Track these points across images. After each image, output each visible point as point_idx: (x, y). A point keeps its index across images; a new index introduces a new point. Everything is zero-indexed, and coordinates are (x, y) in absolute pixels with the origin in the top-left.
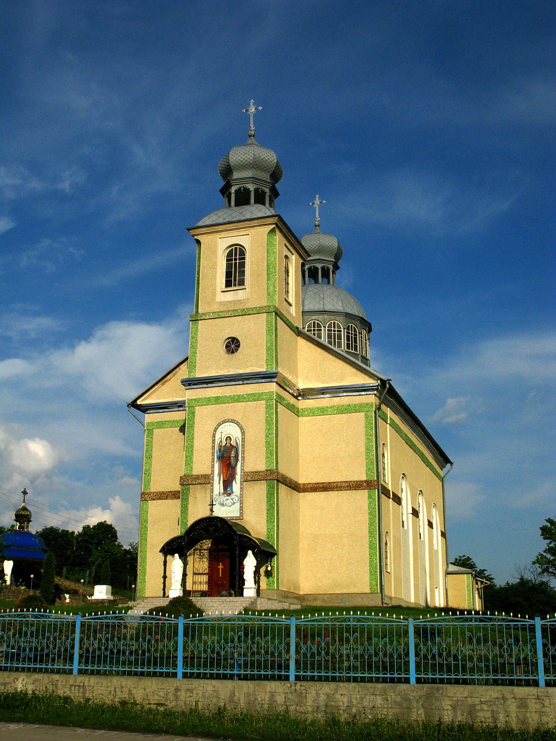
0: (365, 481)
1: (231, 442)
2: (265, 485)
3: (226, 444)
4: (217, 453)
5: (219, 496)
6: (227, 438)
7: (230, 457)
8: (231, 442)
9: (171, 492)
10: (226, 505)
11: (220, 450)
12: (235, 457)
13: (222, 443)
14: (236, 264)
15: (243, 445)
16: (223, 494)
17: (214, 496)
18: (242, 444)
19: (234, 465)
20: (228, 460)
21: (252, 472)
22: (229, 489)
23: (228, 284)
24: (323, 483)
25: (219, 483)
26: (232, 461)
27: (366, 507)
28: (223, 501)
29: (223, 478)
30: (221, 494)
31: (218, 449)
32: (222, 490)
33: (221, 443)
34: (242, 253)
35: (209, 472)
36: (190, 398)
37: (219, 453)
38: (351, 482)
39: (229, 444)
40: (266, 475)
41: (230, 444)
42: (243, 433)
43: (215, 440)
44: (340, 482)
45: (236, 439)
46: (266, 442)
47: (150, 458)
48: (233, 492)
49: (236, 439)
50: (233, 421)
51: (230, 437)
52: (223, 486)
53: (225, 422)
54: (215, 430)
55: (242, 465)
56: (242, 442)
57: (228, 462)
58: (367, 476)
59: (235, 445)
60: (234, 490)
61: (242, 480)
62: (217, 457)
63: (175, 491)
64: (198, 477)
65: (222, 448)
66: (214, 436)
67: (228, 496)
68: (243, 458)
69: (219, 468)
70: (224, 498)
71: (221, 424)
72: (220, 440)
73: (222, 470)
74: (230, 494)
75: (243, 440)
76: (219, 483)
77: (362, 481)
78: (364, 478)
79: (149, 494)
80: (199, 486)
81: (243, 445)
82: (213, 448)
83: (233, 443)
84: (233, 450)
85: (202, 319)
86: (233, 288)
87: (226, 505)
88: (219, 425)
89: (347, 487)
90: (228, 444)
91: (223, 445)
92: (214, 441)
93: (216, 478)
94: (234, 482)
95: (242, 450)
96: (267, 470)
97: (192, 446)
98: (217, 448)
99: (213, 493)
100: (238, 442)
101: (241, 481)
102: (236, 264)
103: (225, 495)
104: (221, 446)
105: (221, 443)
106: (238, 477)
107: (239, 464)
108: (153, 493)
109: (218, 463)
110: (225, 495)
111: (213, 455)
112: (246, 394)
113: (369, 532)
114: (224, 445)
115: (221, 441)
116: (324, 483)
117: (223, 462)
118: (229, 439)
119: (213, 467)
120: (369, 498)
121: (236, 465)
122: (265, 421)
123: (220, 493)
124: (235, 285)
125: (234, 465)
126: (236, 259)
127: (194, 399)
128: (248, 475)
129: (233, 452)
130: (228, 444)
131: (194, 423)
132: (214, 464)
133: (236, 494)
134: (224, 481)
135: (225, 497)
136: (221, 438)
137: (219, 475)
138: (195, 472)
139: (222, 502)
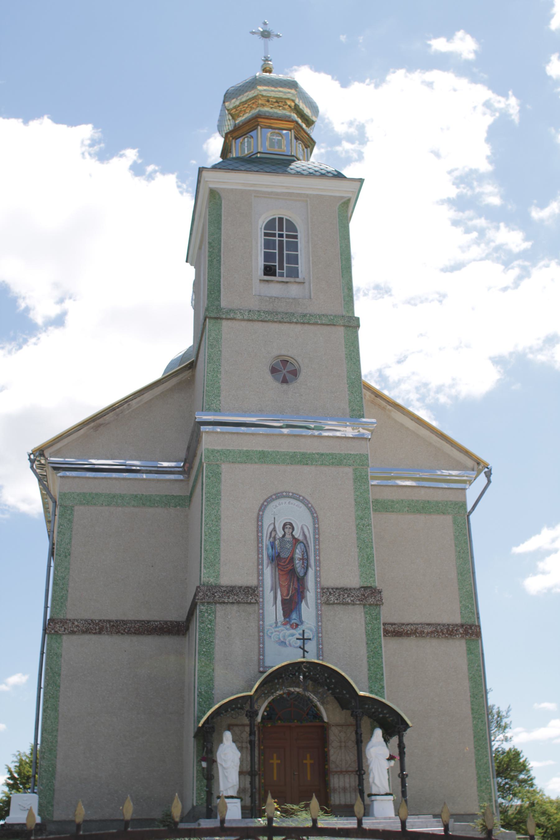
0: (462, 626)
1: (294, 533)
2: (363, 614)
3: (284, 536)
4: (268, 549)
5: (276, 626)
6: (285, 525)
7: (292, 559)
8: (294, 533)
9: (109, 621)
10: (290, 645)
11: (273, 545)
12: (303, 559)
13: (276, 534)
14: (281, 242)
15: (317, 540)
16: (285, 624)
17: (267, 628)
18: (315, 538)
19: (302, 574)
20: (289, 563)
21: (337, 589)
22: (294, 616)
23: (269, 271)
24: (392, 624)
25: (275, 603)
26: (297, 566)
27: (465, 667)
28: (284, 637)
29: (282, 595)
30: (279, 624)
31: (268, 543)
32: (281, 618)
33: (273, 535)
34: (291, 226)
35: (252, 581)
36: (210, 447)
37: (270, 550)
38: (439, 625)
39: (291, 536)
40: (364, 595)
41: (293, 536)
42: (316, 519)
43: (262, 525)
44: (421, 624)
45: (302, 528)
46: (358, 538)
47: (66, 557)
48: (302, 622)
49: (302, 528)
50: (296, 497)
51: (291, 524)
52: (283, 609)
53: (279, 496)
54: (263, 508)
55: (317, 576)
56: (314, 535)
57: (290, 567)
58: (462, 617)
59: (301, 538)
60: (304, 618)
61: (319, 601)
62: (268, 556)
63: (117, 621)
64: (231, 590)
65: (277, 542)
66: (260, 519)
67: (293, 628)
68: (318, 563)
69: (274, 577)
70: (286, 631)
71: (273, 500)
72: (272, 527)
73: (279, 579)
74: (297, 625)
75: (317, 531)
76: (275, 603)
77: (457, 625)
78: (458, 620)
79: (64, 622)
80: (235, 607)
81: (317, 540)
82: (259, 540)
83: (297, 534)
84: (299, 547)
85: (228, 317)
86: (277, 278)
87: (290, 645)
88: (269, 500)
89: (432, 632)
90: (288, 537)
91: (277, 537)
92: (259, 528)
93: (268, 595)
94: (303, 604)
95: (315, 549)
96: (365, 588)
97: (217, 533)
98: (266, 541)
99: (263, 621)
100: (307, 533)
101: (317, 603)
102: (281, 242)
103: (288, 627)
104: (275, 538)
105: (273, 535)
106: (311, 595)
107: (311, 573)
108: (73, 621)
109: (269, 569)
110: (288, 627)
111: (259, 551)
112: (318, 454)
113: (472, 709)
114: (281, 536)
115: (274, 529)
116: (395, 624)
117: (280, 567)
118: (288, 526)
119: (260, 574)
120: (468, 654)
121: (306, 573)
122: (353, 503)
123: (276, 623)
124: (282, 275)
125: (302, 574)
126: (281, 236)
127: (218, 451)
128: (330, 593)
129: (297, 551)
130: (288, 537)
131: (219, 492)
132: (262, 569)
133: (308, 626)
134: (284, 602)
135: (287, 629)
136: (274, 523)
137: (274, 589)
138: (226, 580)
139: (282, 639)
